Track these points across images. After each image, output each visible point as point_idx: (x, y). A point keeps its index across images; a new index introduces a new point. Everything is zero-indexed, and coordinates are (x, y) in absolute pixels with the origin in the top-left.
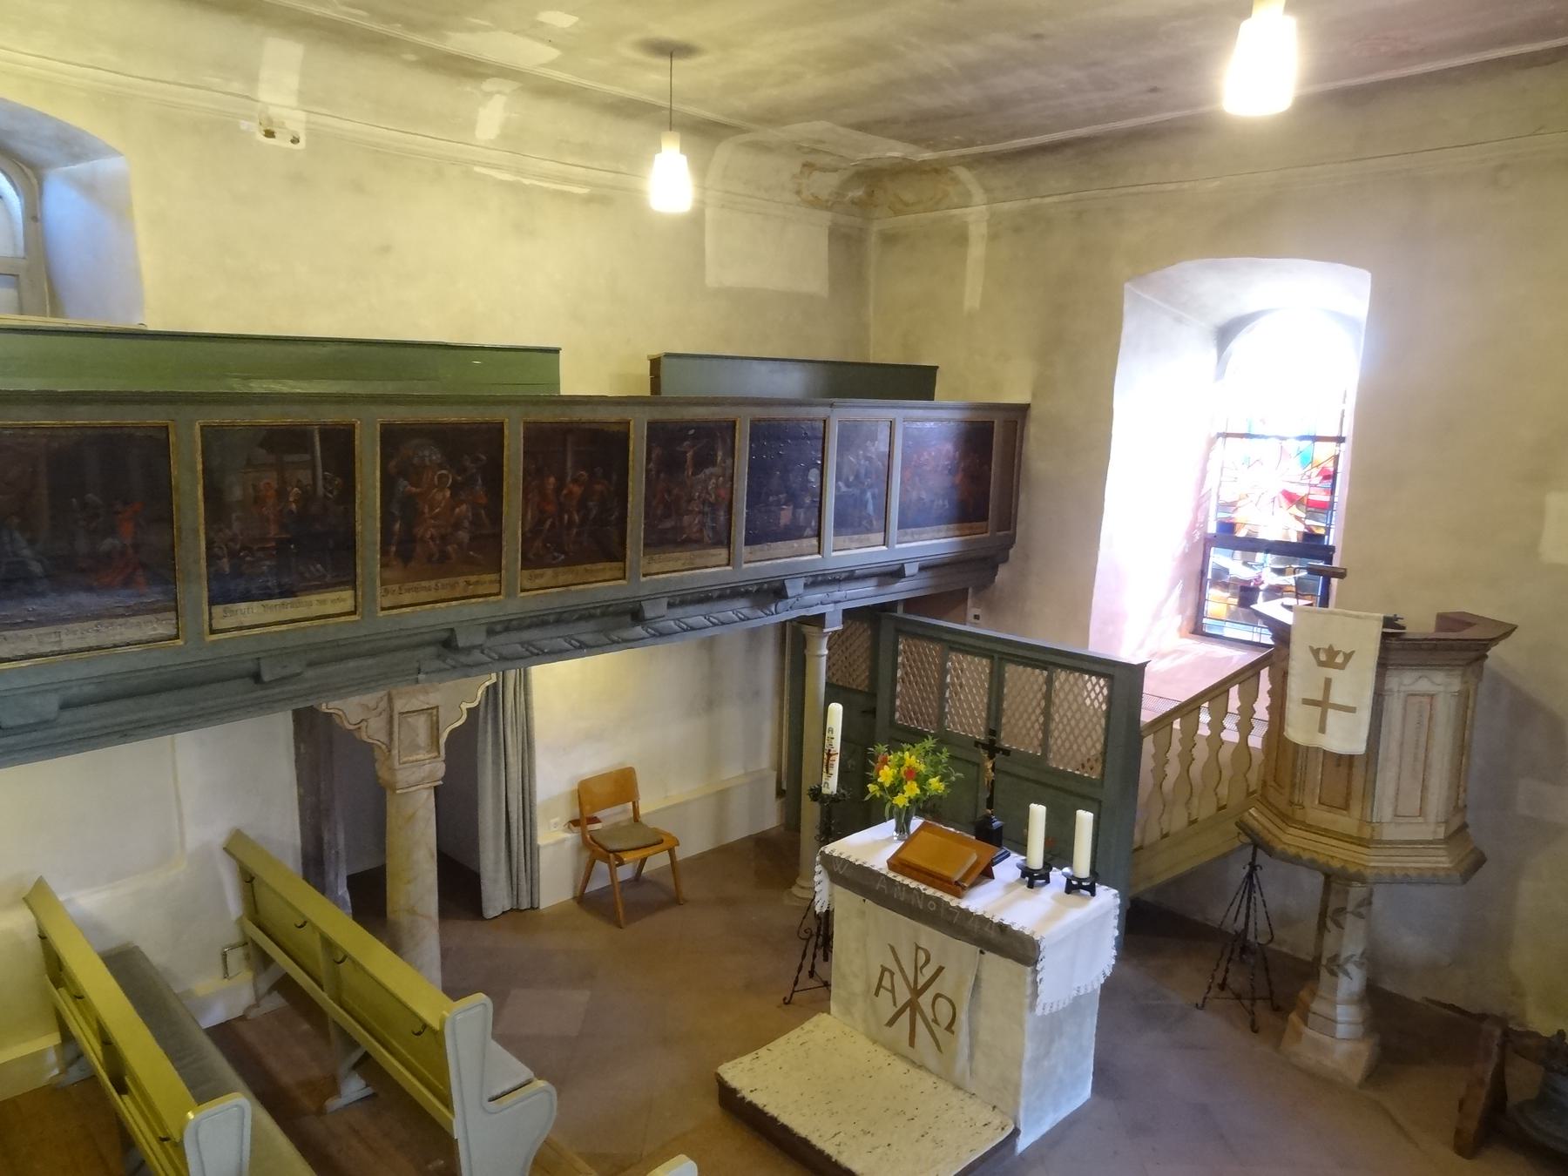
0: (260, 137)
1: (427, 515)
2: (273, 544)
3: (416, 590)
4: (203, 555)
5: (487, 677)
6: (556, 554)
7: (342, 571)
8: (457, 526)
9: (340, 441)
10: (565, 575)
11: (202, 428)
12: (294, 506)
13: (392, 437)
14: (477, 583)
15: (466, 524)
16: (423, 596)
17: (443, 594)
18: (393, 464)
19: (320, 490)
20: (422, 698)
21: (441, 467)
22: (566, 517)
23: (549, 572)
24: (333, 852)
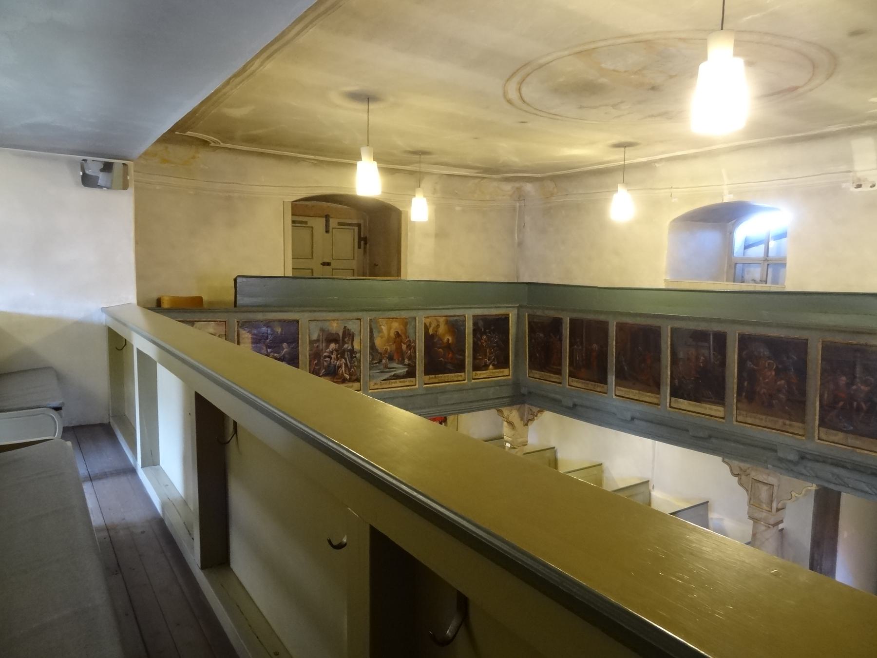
0: (853, 189)
2: (693, 378)
3: (755, 418)
4: (669, 377)
5: (810, 484)
6: (846, 425)
7: (719, 398)
8: (779, 391)
9: (721, 339)
10: (852, 440)
11: (671, 328)
12: (702, 365)
13: (745, 341)
16: (757, 422)
17: (770, 425)
18: (744, 353)
19: (712, 360)
20: (765, 477)
21: (769, 358)
22: (855, 404)
24: (818, 567)
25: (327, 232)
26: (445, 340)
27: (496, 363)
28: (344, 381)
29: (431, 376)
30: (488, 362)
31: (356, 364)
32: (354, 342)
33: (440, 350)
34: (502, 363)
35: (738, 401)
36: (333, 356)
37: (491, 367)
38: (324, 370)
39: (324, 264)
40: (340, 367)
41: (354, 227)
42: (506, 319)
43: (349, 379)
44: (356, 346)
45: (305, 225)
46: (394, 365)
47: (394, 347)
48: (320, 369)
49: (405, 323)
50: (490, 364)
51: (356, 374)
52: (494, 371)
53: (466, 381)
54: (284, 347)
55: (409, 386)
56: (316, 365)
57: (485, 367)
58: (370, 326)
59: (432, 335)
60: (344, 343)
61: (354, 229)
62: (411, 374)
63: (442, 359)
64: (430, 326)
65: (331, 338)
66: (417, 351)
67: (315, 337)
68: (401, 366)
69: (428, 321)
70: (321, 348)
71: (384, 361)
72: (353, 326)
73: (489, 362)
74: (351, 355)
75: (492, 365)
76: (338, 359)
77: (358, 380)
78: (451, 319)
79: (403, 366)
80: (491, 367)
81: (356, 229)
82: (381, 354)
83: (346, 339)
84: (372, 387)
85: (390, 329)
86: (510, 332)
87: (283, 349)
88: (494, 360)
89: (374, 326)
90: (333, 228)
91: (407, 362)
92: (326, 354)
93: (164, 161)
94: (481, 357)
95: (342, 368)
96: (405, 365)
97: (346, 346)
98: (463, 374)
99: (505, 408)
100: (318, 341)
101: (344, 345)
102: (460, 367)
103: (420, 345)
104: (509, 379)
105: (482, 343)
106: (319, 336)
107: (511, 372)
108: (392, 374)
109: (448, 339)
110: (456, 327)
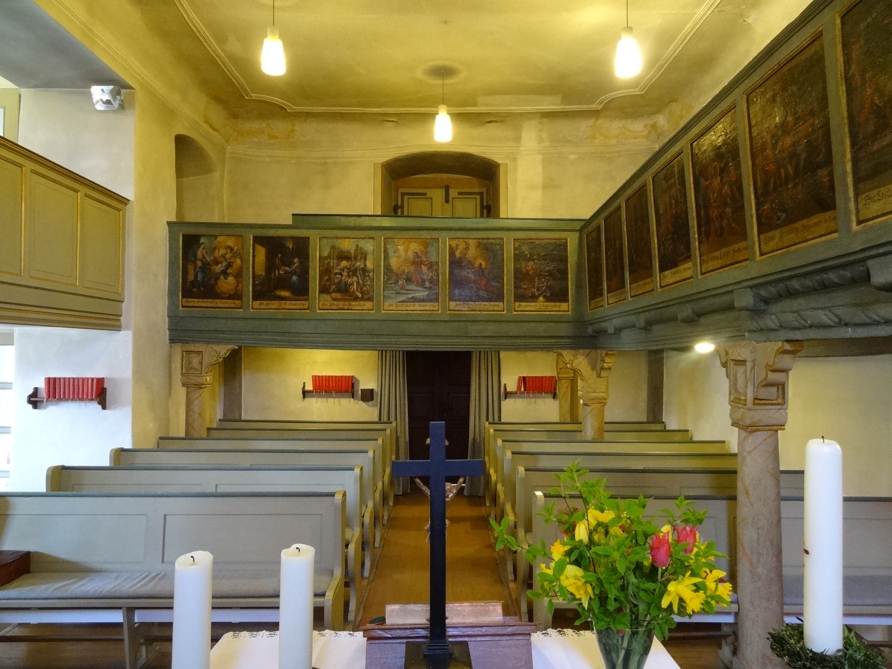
1: (712, 200)
3: (712, 259)
4: (656, 246)
14: (739, 250)
15: (729, 201)
22: (782, 171)
23: (777, 233)
25: (447, 201)
26: (477, 264)
27: (548, 295)
28: (356, 299)
30: (537, 293)
31: (369, 283)
34: (560, 296)
35: (700, 243)
36: (345, 274)
37: (541, 299)
40: (352, 284)
43: (362, 297)
44: (369, 265)
45: (423, 197)
46: (413, 287)
48: (330, 285)
50: (539, 296)
51: (369, 293)
53: (505, 312)
56: (327, 281)
57: (534, 298)
59: (460, 258)
61: (476, 198)
64: (457, 249)
65: (343, 256)
66: (440, 275)
68: (420, 288)
69: (454, 243)
70: (332, 264)
71: (400, 282)
72: (368, 246)
74: (364, 273)
75: (543, 297)
76: (349, 276)
77: (370, 299)
78: (484, 241)
80: (541, 299)
81: (478, 197)
82: (397, 275)
84: (387, 308)
85: (406, 251)
86: (569, 260)
88: (545, 291)
90: (453, 198)
92: (337, 271)
93: (272, 137)
94: (525, 286)
97: (359, 263)
98: (501, 304)
100: (329, 257)
104: (568, 314)
105: (527, 271)
106: (330, 253)
108: (410, 296)
109: (481, 264)
110: (491, 250)
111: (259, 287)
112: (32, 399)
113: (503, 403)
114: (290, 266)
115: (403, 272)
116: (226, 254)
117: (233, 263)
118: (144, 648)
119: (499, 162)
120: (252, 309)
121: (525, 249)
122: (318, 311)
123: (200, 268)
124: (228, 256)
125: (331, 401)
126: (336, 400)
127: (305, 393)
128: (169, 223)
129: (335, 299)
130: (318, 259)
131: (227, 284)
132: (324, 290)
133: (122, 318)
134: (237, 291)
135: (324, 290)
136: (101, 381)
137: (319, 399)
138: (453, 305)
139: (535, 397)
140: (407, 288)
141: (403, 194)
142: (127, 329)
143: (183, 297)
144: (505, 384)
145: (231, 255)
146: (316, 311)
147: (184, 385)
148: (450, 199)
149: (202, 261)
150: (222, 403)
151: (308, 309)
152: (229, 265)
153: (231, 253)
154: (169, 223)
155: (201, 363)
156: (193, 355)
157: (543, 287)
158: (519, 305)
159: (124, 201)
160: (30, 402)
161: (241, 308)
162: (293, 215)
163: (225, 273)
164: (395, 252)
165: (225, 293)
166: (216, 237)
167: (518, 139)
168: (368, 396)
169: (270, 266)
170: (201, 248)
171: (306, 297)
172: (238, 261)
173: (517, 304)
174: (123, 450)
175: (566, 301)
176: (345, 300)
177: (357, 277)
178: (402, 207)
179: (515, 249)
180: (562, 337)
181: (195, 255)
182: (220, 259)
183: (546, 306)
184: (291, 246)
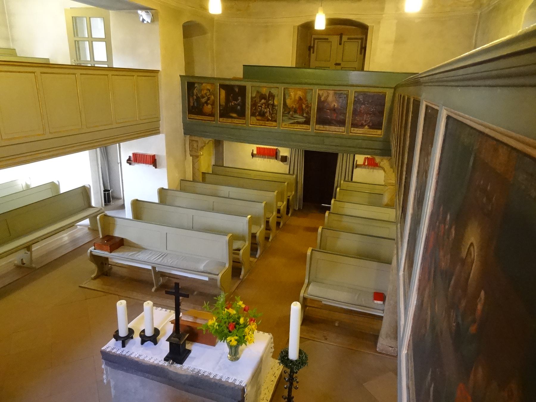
25: (340, 44)
26: (332, 105)
27: (371, 125)
28: (268, 120)
29: (320, 126)
30: (364, 124)
31: (275, 112)
32: (275, 100)
33: (328, 111)
34: (377, 126)
36: (263, 107)
37: (366, 127)
38: (258, 113)
39: (337, 64)
41: (358, 41)
42: (384, 96)
44: (276, 103)
47: (297, 106)
48: (256, 112)
49: (306, 92)
50: (366, 125)
52: (369, 130)
53: (345, 133)
54: (239, 99)
55: (305, 129)
57: (362, 126)
58: (284, 92)
60: (269, 100)
62: (307, 122)
63: (328, 117)
64: (322, 95)
65: (262, 97)
67: (254, 95)
68: (301, 117)
71: (291, 113)
73: (365, 123)
74: (273, 107)
76: (265, 108)
77: (275, 121)
79: (302, 117)
80: (366, 127)
81: (360, 41)
82: (289, 109)
83: (270, 98)
84: (283, 126)
85: (295, 95)
87: (239, 100)
88: (369, 122)
89: (286, 92)
90: (344, 42)
91: (305, 115)
92: (259, 105)
95: (267, 114)
96: (304, 117)
97: (270, 102)
98: (344, 128)
99: (377, 157)
100: (255, 97)
101: (269, 101)
102: (342, 123)
103: (315, 107)
104: (381, 137)
105: (360, 111)
107: (382, 132)
108: (296, 121)
109: (335, 105)
111: (222, 111)
112: (128, 162)
113: (355, 170)
114: (236, 101)
115: (293, 107)
116: (207, 93)
117: (210, 98)
118: (161, 278)
119: (369, 25)
120: (219, 122)
121: (361, 98)
122: (250, 125)
123: (196, 99)
124: (208, 94)
125: (266, 160)
126: (268, 160)
127: (253, 155)
128: (180, 76)
129: (258, 120)
130: (250, 98)
131: (208, 108)
132: (253, 114)
133: (160, 128)
134: (212, 112)
135: (253, 114)
136: (154, 156)
137: (260, 159)
138: (318, 127)
139: (373, 169)
140: (294, 116)
141: (315, 39)
142: (163, 133)
143: (188, 114)
144: (357, 160)
145: (209, 93)
146: (249, 126)
147: (191, 156)
148: (343, 43)
149: (196, 96)
150: (214, 157)
151: (245, 124)
152: (209, 99)
153: (209, 92)
154: (180, 76)
155: (198, 146)
156: (194, 142)
157: (368, 120)
158: (354, 130)
159: (157, 72)
160: (127, 162)
161: (214, 121)
162: (243, 65)
163: (206, 103)
164: (289, 96)
165: (207, 113)
166: (202, 84)
167: (383, 9)
168: (284, 159)
169: (227, 100)
170: (195, 89)
171: (244, 118)
172: (213, 97)
173: (352, 129)
174: (163, 189)
175: (381, 129)
176: (264, 121)
177: (269, 109)
178: (313, 47)
179: (355, 97)
180: (376, 149)
181: (193, 93)
182: (205, 95)
183: (369, 131)
184: (237, 91)
